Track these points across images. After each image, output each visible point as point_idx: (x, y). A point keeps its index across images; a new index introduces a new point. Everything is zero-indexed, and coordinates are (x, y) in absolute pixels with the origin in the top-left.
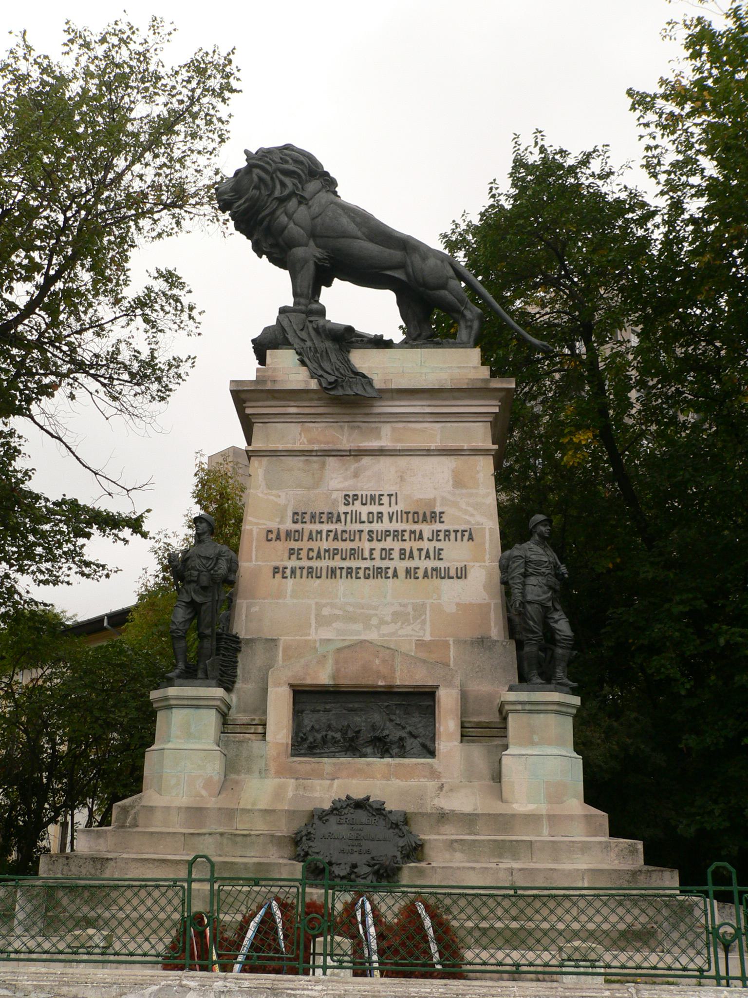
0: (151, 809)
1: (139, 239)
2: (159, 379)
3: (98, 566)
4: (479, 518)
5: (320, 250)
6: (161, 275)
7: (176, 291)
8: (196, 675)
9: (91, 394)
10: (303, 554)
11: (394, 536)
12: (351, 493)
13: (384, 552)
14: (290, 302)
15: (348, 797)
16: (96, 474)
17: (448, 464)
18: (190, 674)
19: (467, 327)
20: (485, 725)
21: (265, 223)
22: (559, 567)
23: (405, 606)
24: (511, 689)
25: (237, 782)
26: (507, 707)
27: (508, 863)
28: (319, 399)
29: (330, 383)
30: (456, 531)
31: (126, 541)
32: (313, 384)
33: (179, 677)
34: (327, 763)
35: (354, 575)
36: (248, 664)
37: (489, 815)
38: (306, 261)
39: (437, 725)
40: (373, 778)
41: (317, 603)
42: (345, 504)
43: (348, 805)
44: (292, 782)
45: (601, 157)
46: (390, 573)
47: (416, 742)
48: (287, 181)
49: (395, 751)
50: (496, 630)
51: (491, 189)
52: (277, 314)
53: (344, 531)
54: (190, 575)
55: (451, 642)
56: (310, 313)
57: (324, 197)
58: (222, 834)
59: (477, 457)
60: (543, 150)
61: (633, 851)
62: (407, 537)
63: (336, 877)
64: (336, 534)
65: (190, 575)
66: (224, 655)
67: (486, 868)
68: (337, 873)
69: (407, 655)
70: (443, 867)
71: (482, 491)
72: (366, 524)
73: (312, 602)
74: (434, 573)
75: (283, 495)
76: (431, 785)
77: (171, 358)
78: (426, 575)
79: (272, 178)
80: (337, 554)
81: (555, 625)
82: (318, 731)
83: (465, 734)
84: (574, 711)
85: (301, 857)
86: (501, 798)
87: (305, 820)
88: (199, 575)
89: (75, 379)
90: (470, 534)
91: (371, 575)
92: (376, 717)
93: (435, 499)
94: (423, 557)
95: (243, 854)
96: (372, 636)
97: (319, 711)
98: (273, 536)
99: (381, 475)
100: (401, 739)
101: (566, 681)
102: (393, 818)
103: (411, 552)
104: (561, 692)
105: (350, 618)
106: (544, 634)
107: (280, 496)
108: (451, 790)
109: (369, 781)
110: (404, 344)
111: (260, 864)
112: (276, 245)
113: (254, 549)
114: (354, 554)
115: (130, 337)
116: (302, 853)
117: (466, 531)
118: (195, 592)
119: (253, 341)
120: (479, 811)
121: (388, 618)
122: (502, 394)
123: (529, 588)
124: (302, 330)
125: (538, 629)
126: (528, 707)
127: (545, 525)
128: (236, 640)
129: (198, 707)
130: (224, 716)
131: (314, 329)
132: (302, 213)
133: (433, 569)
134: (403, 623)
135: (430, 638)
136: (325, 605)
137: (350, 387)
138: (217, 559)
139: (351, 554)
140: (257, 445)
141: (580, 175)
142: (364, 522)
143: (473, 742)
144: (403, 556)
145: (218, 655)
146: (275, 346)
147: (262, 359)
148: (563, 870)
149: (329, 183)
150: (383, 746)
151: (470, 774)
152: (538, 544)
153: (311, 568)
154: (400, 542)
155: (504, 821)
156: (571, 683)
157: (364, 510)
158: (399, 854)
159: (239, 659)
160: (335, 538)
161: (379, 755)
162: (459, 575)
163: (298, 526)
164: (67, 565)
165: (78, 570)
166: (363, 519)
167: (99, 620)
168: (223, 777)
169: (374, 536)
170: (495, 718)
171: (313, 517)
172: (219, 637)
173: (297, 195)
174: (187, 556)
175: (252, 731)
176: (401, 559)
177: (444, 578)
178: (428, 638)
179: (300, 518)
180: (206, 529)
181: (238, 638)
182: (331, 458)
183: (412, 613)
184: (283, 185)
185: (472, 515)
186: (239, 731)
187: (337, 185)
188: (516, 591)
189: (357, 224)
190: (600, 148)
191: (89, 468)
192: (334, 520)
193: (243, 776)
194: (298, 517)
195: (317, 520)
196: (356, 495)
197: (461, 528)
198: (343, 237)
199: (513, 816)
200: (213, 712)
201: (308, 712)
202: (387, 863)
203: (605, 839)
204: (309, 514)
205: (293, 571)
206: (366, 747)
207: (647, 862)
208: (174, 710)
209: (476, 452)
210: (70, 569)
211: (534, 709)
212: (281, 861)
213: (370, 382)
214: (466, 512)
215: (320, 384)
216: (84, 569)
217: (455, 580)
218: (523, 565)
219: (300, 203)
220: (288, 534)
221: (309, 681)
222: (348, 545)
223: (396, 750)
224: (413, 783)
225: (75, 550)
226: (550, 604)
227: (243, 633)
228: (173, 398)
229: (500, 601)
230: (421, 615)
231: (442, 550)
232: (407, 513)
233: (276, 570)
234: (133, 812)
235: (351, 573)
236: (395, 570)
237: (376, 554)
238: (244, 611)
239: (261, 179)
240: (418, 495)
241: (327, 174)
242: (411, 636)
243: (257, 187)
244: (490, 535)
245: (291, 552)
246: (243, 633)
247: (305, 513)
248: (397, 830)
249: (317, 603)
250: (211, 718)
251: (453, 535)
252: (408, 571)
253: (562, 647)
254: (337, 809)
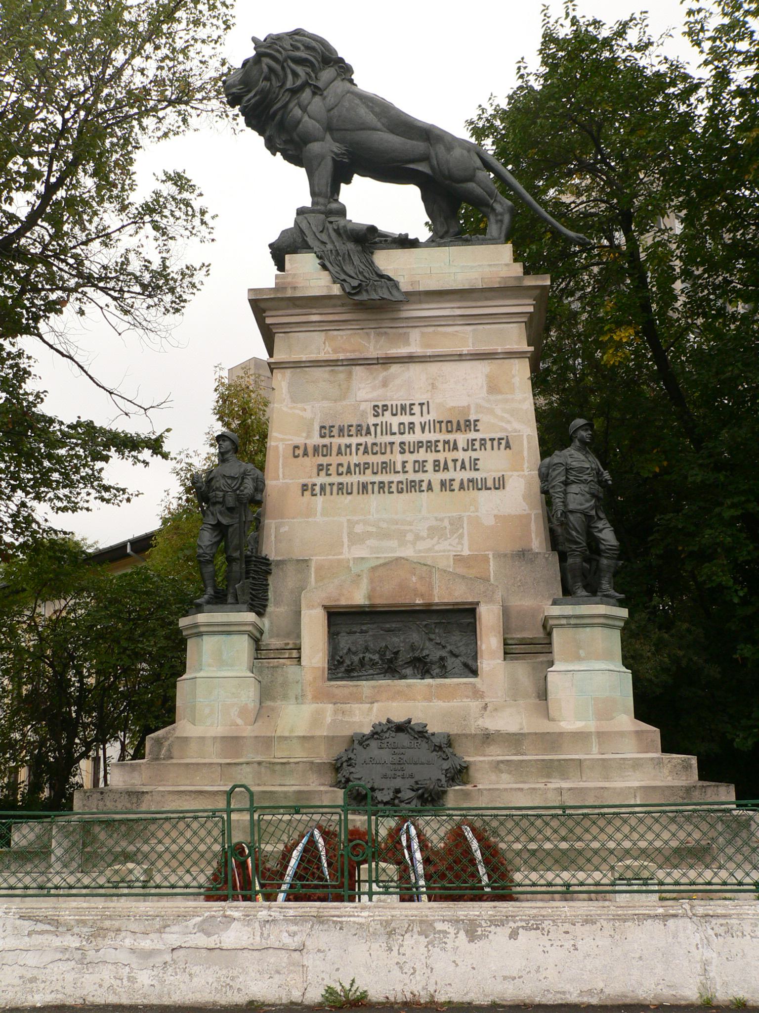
0: (186, 740)
1: (143, 140)
2: (172, 290)
3: (118, 490)
4: (516, 425)
5: (338, 144)
6: (169, 178)
7: (185, 195)
8: (226, 600)
9: (101, 308)
10: (333, 470)
11: (427, 447)
12: (380, 404)
13: (417, 464)
14: (307, 202)
15: (389, 721)
16: (111, 393)
17: (482, 368)
18: (220, 599)
19: (497, 221)
20: (528, 641)
21: (278, 117)
22: (602, 474)
23: (442, 520)
24: (555, 603)
25: (273, 709)
26: (551, 622)
27: (556, 783)
28: (343, 305)
29: (354, 288)
30: (492, 440)
31: (146, 463)
32: (336, 290)
33: (208, 603)
34: (366, 686)
35: (386, 490)
36: (279, 587)
37: (536, 734)
38: (323, 157)
39: (479, 643)
40: (414, 700)
41: (348, 520)
42: (375, 416)
43: (388, 729)
44: (329, 708)
45: (639, 26)
46: (425, 486)
47: (457, 662)
48: (299, 70)
49: (436, 670)
50: (537, 542)
51: (519, 68)
52: (295, 215)
53: (374, 444)
54: (215, 497)
55: (491, 556)
56: (329, 213)
57: (340, 86)
58: (259, 763)
59: (512, 360)
60: (574, 21)
61: (687, 767)
62: (440, 447)
63: (379, 802)
64: (366, 447)
65: (215, 497)
66: (254, 578)
67: (534, 789)
68: (379, 799)
69: (445, 571)
70: (490, 789)
71: (519, 396)
72: (398, 436)
73: (344, 520)
74: (471, 484)
75: (308, 407)
76: (474, 705)
77: (184, 268)
78: (462, 487)
79: (283, 68)
80: (368, 468)
81: (599, 535)
82: (355, 653)
83: (508, 651)
84: (622, 624)
85: (343, 783)
86: (547, 716)
87: (344, 746)
88: (224, 496)
89: (84, 294)
90: (507, 442)
91: (405, 489)
92: (415, 637)
93: (469, 407)
94: (458, 468)
95: (282, 782)
96: (408, 552)
97: (355, 632)
98: (300, 452)
99: (409, 384)
100: (442, 659)
101: (612, 592)
102: (436, 741)
103: (446, 463)
104: (608, 604)
105: (385, 535)
106: (588, 544)
107: (305, 410)
108: (496, 710)
109: (411, 704)
110: (431, 242)
111: (300, 792)
112: (290, 141)
113: (281, 466)
114: (385, 468)
115: (140, 246)
116: (343, 780)
117: (503, 439)
118: (220, 513)
119: (271, 246)
120: (525, 731)
121: (424, 534)
122: (538, 292)
123: (570, 497)
124: (322, 232)
125: (581, 539)
126: (573, 621)
127: (586, 430)
128: (266, 562)
129: (229, 633)
130: (257, 642)
131: (334, 230)
132: (316, 105)
133: (469, 481)
134: (439, 539)
135: (469, 553)
136: (357, 522)
137: (375, 290)
138: (243, 478)
139: (382, 468)
140: (279, 356)
141: (615, 47)
142: (395, 434)
143: (517, 659)
144: (437, 468)
145: (247, 578)
146: (294, 250)
147: (281, 266)
148: (615, 789)
149: (344, 70)
150: (423, 667)
151: (515, 693)
152: (579, 450)
153: (341, 484)
154: (434, 453)
156: (617, 594)
157: (395, 421)
158: (443, 778)
159: (270, 582)
160: (366, 452)
161: (419, 676)
162: (497, 486)
163: (326, 441)
164: (86, 490)
165: (97, 495)
166: (393, 431)
167: (122, 547)
168: (258, 705)
169: (407, 448)
170: (540, 634)
171: (341, 430)
172: (248, 560)
173: (310, 85)
174: (211, 476)
175: (287, 656)
176: (435, 471)
177: (481, 489)
178: (466, 552)
179: (327, 432)
180: (230, 447)
181: (268, 560)
182: (358, 368)
183: (449, 527)
184: (295, 75)
185: (509, 422)
186: (272, 656)
187: (353, 73)
188: (557, 500)
189: (376, 114)
190: (637, 16)
191: (103, 388)
192: (364, 432)
193: (279, 703)
194: (325, 431)
195: (346, 434)
196: (386, 406)
197: (497, 436)
198: (361, 129)
199: (561, 734)
200: (246, 637)
201: (344, 634)
202: (432, 787)
203: (658, 755)
204: (337, 427)
205: (323, 488)
206: (405, 668)
207: (701, 778)
208: (205, 637)
210: (89, 494)
211: (579, 623)
212: (322, 788)
213: (396, 285)
214: (502, 419)
215: (344, 289)
216: (103, 493)
217: (493, 491)
218: (564, 473)
219: (314, 94)
220: (316, 449)
221: (343, 602)
222: (379, 459)
223: (437, 671)
224: (455, 704)
225: (93, 474)
226: (593, 513)
227: (273, 554)
228: (188, 309)
229: (540, 511)
230: (458, 530)
231: (478, 459)
232: (440, 422)
233: (304, 488)
234: (167, 743)
235: (383, 488)
236: (430, 483)
237: (409, 467)
238: (273, 531)
239: (271, 69)
240: (451, 404)
241: (341, 60)
242: (449, 551)
243: (267, 79)
244: (529, 443)
245: (320, 468)
246: (273, 554)
247: (333, 427)
248: (440, 753)
249: (348, 520)
250: (243, 644)
251: (489, 444)
252: (443, 484)
253: (607, 558)
254: (377, 734)
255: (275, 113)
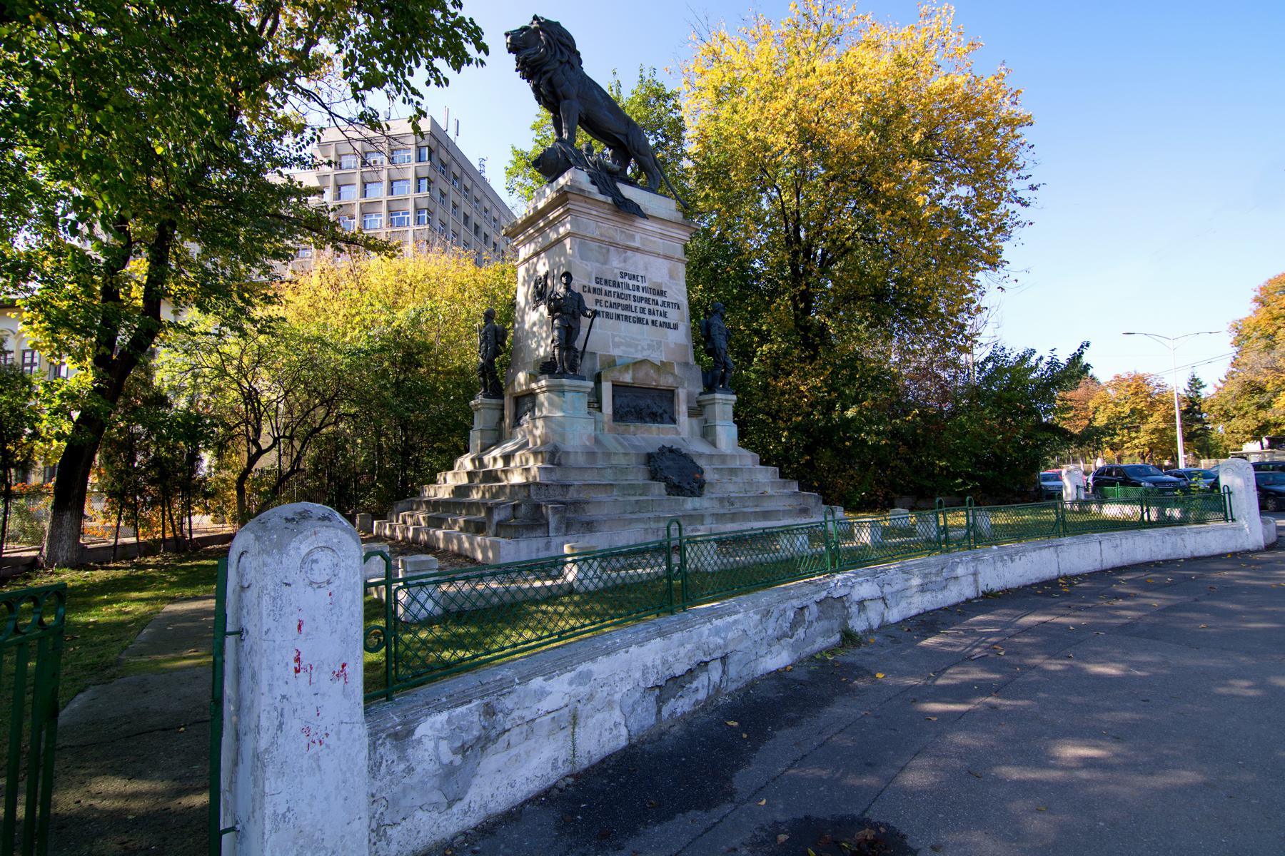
21: (549, 75)
36: (586, 366)
50: (691, 360)
105: (629, 345)
150: (655, 417)
155: (723, 458)
157: (631, 283)
163: (598, 286)
194: (598, 280)
209: (679, 260)
241: (579, 54)
255: (547, 72)
